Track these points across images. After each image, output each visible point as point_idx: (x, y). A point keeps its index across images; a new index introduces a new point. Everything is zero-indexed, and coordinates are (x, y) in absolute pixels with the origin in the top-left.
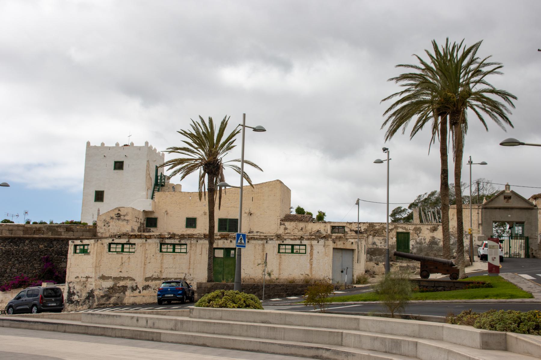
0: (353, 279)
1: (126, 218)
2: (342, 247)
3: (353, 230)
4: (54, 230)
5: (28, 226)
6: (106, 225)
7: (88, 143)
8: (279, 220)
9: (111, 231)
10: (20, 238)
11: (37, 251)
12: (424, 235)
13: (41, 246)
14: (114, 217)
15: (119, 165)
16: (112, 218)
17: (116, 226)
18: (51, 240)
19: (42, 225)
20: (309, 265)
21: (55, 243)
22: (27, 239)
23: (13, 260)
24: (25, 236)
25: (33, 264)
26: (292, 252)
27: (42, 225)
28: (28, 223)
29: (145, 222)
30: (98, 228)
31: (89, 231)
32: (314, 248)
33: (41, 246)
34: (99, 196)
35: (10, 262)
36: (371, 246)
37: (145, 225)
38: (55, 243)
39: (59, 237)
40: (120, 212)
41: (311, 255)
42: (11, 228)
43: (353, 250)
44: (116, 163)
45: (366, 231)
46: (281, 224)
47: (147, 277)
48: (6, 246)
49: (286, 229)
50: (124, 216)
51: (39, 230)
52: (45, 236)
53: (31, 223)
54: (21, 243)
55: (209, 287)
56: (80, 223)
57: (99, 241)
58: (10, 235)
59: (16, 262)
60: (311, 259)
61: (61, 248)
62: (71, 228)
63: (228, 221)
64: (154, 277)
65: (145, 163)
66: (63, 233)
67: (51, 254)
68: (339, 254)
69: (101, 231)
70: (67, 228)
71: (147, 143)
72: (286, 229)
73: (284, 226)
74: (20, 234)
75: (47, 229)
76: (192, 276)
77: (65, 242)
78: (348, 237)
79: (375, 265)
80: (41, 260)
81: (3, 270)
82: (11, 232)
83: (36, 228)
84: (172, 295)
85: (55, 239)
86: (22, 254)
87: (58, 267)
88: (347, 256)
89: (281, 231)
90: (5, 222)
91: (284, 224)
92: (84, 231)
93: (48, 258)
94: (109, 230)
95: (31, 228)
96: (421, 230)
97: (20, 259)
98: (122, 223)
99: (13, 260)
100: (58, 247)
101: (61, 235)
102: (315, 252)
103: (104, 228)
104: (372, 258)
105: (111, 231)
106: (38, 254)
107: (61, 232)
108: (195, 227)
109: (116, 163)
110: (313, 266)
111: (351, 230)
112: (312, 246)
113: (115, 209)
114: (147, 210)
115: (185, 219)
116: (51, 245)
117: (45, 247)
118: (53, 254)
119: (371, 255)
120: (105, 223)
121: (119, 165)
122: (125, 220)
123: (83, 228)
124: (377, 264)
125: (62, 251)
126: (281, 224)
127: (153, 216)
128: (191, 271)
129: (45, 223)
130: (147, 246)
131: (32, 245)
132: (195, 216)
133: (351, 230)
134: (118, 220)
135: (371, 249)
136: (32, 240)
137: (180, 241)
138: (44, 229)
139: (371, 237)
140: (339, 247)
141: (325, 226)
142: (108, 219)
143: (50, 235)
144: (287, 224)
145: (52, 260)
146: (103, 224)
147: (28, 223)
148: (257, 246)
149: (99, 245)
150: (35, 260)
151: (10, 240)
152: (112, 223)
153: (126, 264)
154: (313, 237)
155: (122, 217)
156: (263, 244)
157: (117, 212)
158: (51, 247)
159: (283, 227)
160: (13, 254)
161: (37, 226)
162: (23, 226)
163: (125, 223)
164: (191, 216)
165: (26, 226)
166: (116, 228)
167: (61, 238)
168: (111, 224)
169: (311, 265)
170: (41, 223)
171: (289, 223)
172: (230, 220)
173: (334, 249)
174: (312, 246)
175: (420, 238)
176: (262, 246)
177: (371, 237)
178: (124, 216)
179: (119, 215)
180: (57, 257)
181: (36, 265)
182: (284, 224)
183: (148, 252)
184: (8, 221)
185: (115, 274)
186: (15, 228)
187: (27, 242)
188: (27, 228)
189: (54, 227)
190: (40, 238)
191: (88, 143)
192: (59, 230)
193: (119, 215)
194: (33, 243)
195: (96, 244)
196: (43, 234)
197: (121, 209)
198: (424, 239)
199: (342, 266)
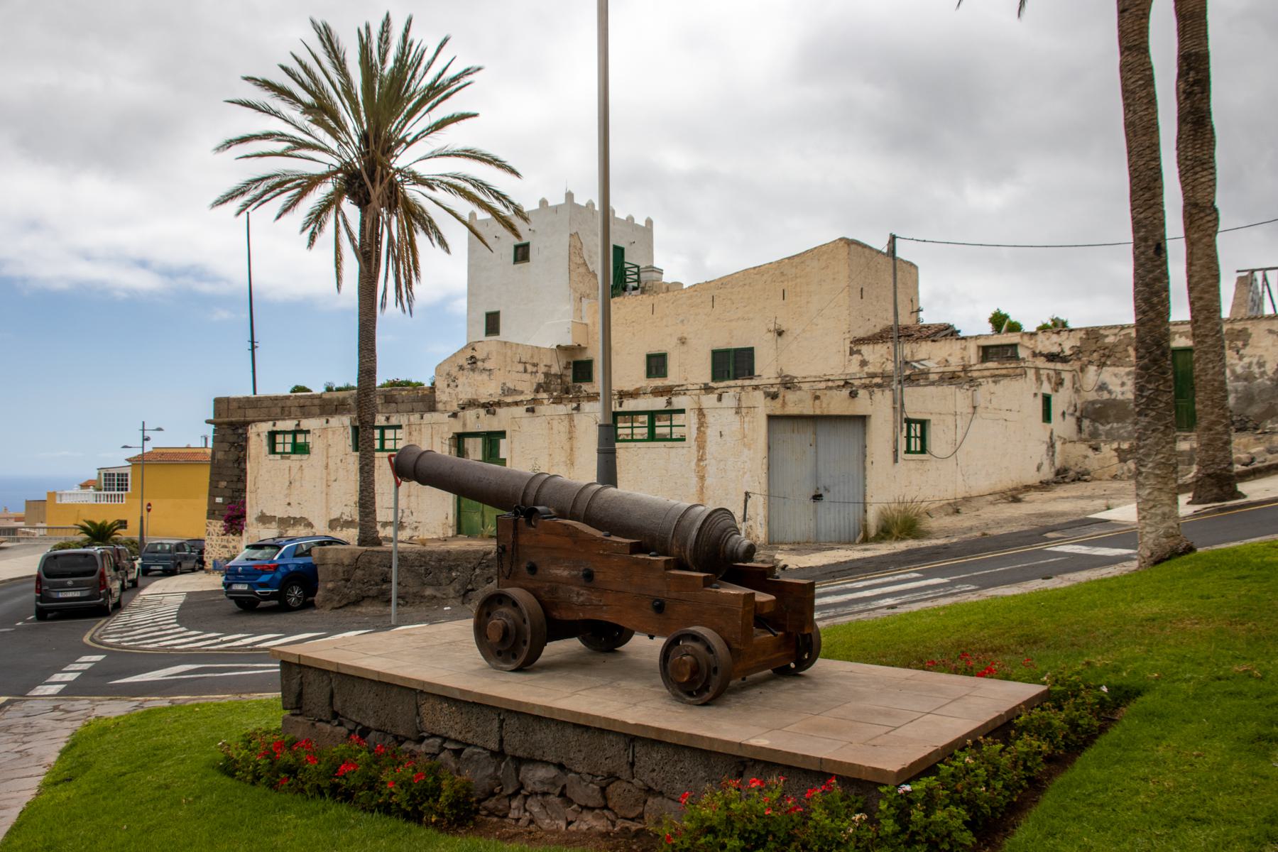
0: (865, 527)
1: (488, 365)
2: (808, 411)
3: (1041, 354)
6: (453, 384)
8: (848, 342)
12: (1259, 352)
16: (461, 368)
20: (694, 480)
26: (652, 437)
29: (570, 372)
30: (438, 393)
32: (710, 419)
34: (493, 323)
36: (1092, 396)
37: (570, 379)
40: (474, 354)
41: (701, 446)
43: (863, 420)
45: (1078, 352)
46: (851, 354)
47: (332, 517)
49: (864, 363)
50: (483, 361)
55: (346, 562)
56: (408, 383)
60: (701, 459)
62: (392, 396)
63: (732, 354)
64: (345, 517)
65: (566, 239)
68: (798, 442)
70: (386, 396)
71: (569, 196)
72: (864, 363)
73: (859, 357)
76: (414, 518)
78: (975, 374)
79: (1090, 453)
84: (245, 587)
88: (836, 444)
89: (854, 368)
91: (859, 352)
92: (414, 401)
94: (457, 395)
96: (1249, 335)
102: (711, 433)
103: (447, 390)
104: (1096, 429)
108: (664, 375)
110: (708, 481)
111: (1035, 355)
112: (701, 412)
114: (563, 344)
115: (644, 358)
119: (1093, 421)
123: (412, 394)
124: (1096, 449)
126: (851, 354)
127: (584, 357)
128: (413, 505)
130: (330, 436)
133: (1035, 355)
134: (473, 370)
135: (1093, 403)
137: (388, 419)
138: (350, 401)
139: (1092, 369)
140: (792, 410)
141: (965, 349)
142: (454, 371)
144: (866, 350)
148: (555, 423)
153: (297, 484)
154: (878, 380)
155: (479, 364)
156: (570, 416)
157: (469, 353)
159: (856, 358)
162: (320, 397)
163: (485, 376)
164: (655, 350)
166: (469, 389)
168: (459, 382)
169: (702, 478)
171: (871, 346)
172: (736, 350)
173: (771, 418)
174: (701, 412)
175: (1246, 360)
176: (566, 423)
177: (1092, 369)
178: (483, 361)
179: (473, 361)
182: (859, 352)
183: (332, 451)
185: (280, 513)
193: (473, 361)
197: (477, 347)
198: (1261, 365)
199: (816, 477)
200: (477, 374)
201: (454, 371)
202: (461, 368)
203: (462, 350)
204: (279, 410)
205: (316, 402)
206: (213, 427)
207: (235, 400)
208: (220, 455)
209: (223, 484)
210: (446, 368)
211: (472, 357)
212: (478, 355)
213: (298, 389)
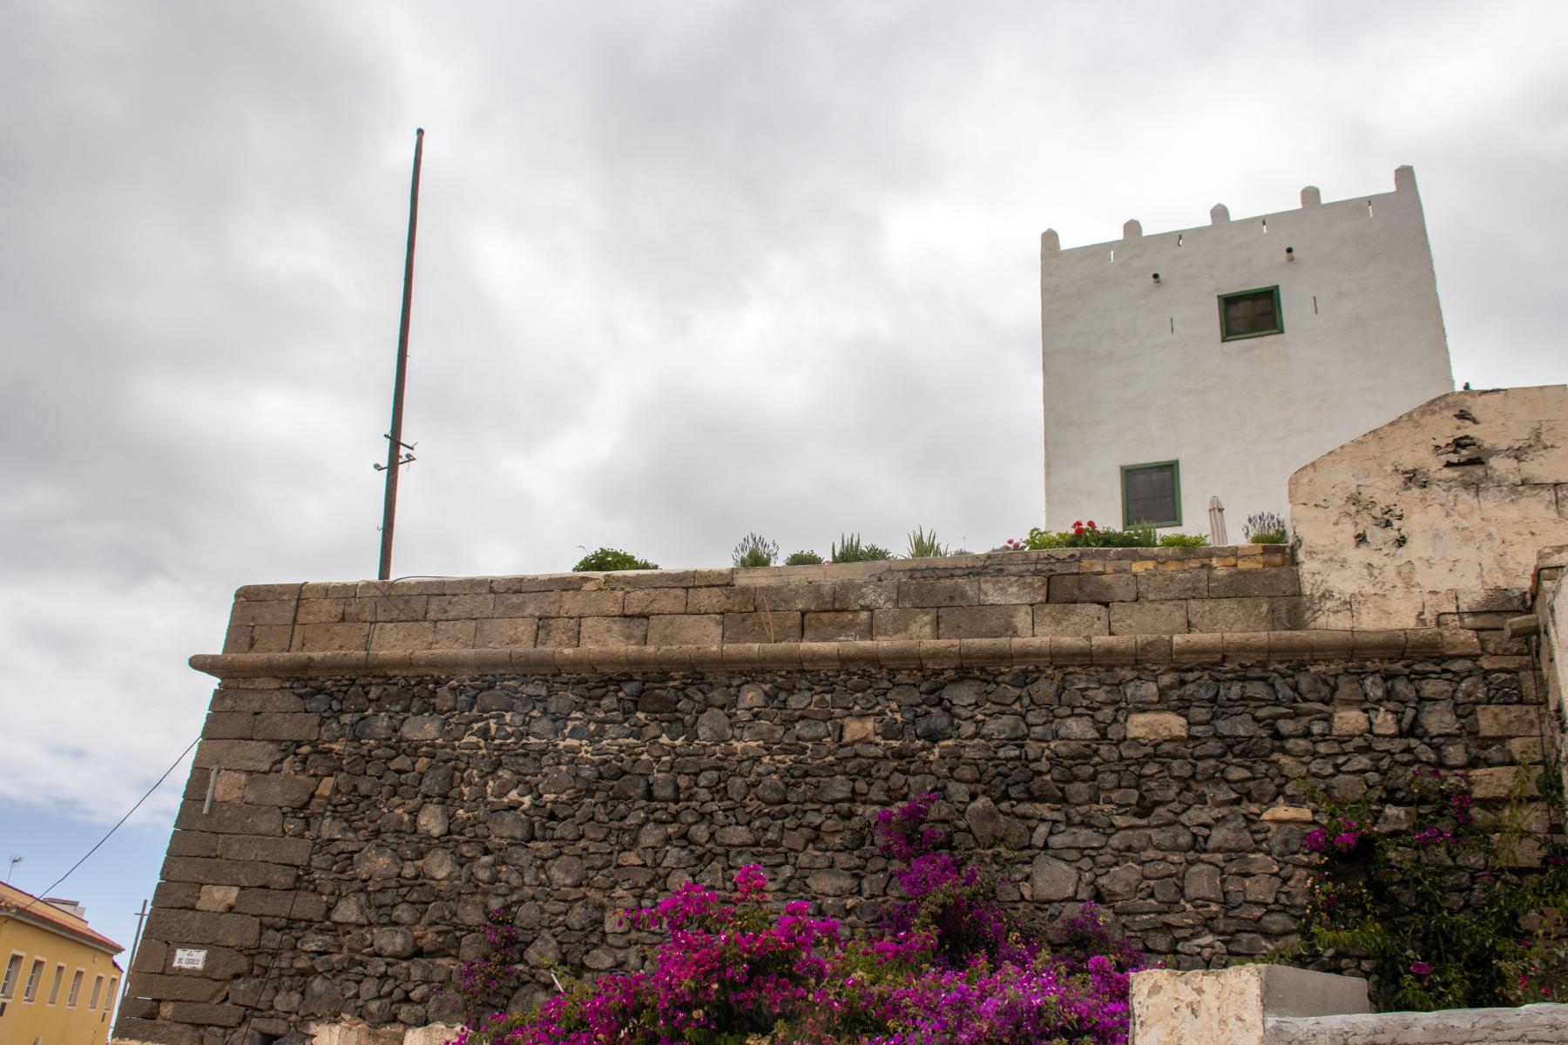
4: (954, 596)
5: (757, 579)
6: (1377, 535)
7: (1050, 238)
9: (1427, 579)
10: (697, 672)
11: (830, 770)
13: (855, 729)
14: (1434, 466)
15: (1251, 313)
16: (1413, 478)
17: (1466, 536)
18: (932, 679)
19: (856, 572)
21: (963, 696)
22: (753, 670)
23: (651, 835)
24: (732, 648)
25: (802, 874)
27: (856, 572)
28: (756, 560)
30: (1308, 567)
31: (1238, 588)
33: (855, 729)
35: (631, 858)
39: (1002, 642)
40: (1471, 430)
42: (637, 600)
44: (1228, 302)
48: (601, 734)
50: (1518, 454)
51: (834, 607)
52: (883, 643)
53: (779, 561)
54: (708, 705)
58: (632, 649)
59: (673, 855)
61: (1018, 741)
66: (1022, 620)
67: (941, 792)
69: (1343, 583)
74: (705, 638)
75: (900, 594)
77: (1044, 689)
80: (860, 839)
81: (577, 916)
82: (637, 628)
83: (815, 589)
85: (968, 669)
86: (719, 790)
87: (1007, 892)
90: (599, 568)
92: (1193, 593)
93: (915, 815)
95: (778, 596)
97: (700, 832)
98: (1512, 513)
99: (651, 835)
100: (992, 726)
105: (1427, 579)
106: (839, 787)
107: (1008, 611)
109: (1228, 302)
113: (1430, 408)
116: (939, 719)
117: (889, 732)
118: (959, 791)
120: (1366, 524)
125: (1024, 760)
129: (875, 555)
131: (788, 723)
134: (1475, 487)
136: (787, 676)
138: (871, 596)
142: (1383, 490)
143: (921, 636)
145: (948, 844)
146: (1348, 530)
147: (756, 560)
150: (816, 836)
151: (629, 688)
152: (1422, 517)
157: (1447, 429)
158: (933, 737)
160: (649, 795)
161: (830, 577)
162: (723, 582)
165: (742, 580)
166: (1467, 553)
170: (850, 555)
180: (990, 816)
181: (823, 883)
184: (626, 561)
187: (751, 696)
188: (738, 596)
189: (950, 572)
190: (845, 661)
191: (1050, 238)
192: (994, 598)
193: (1469, 459)
194: (796, 702)
196: (870, 631)
200: (1491, 505)
203: (1411, 419)
204: (525, 629)
205: (707, 599)
206: (213, 683)
207: (326, 591)
208: (224, 786)
209: (220, 896)
210: (1344, 478)
211: (1459, 444)
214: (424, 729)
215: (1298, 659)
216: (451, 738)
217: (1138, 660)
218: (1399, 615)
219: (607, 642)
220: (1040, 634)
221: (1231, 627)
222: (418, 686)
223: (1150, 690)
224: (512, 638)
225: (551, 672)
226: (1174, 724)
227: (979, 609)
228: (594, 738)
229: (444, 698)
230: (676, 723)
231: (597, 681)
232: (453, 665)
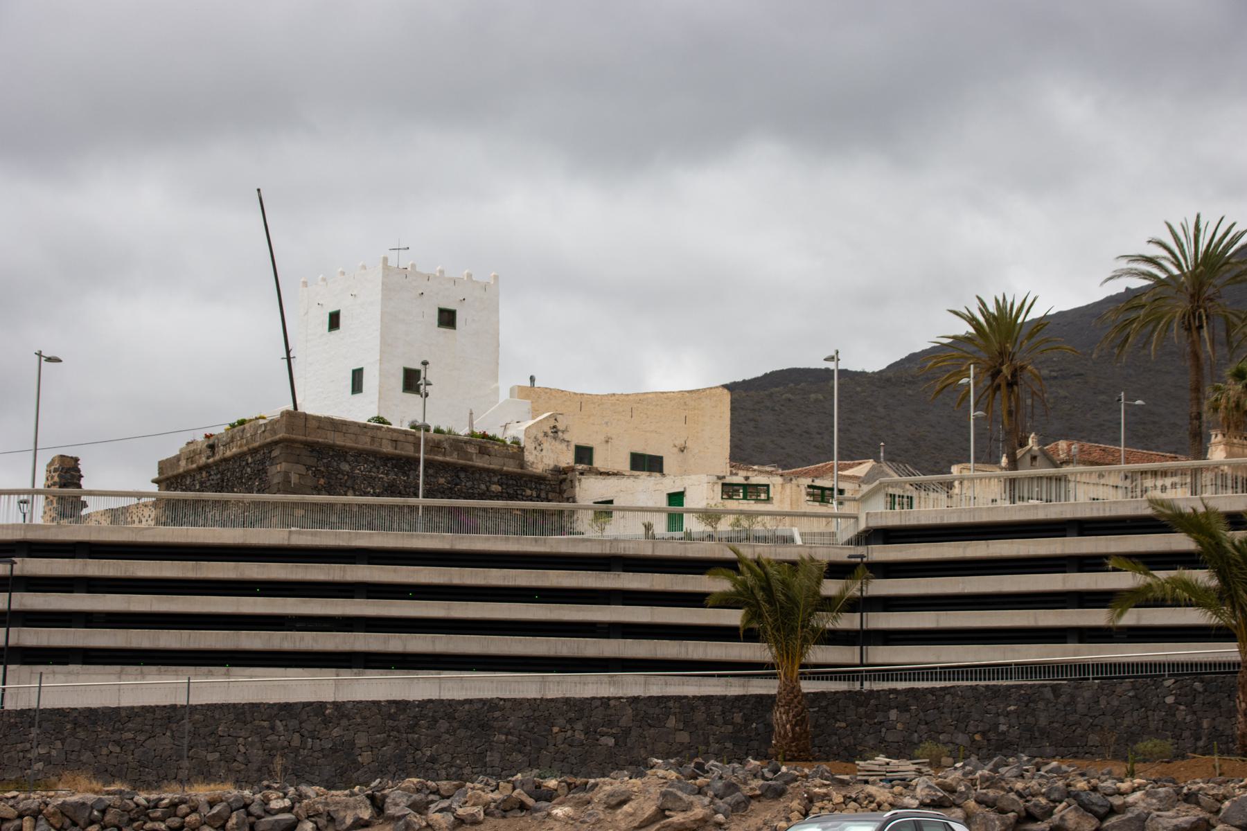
1: (566, 437)
14: (549, 432)
21: (462, 475)
30: (526, 453)
31: (513, 456)
33: (442, 481)
34: (412, 381)
38: (462, 475)
57: (794, 481)
70: (480, 447)
75: (451, 445)
85: (464, 469)
92: (505, 456)
101: (471, 459)
103: (535, 452)
105: (546, 461)
121: (447, 318)
122: (564, 440)
132: (590, 444)
134: (555, 438)
138: (446, 445)
149: (794, 488)
155: (560, 434)
157: (552, 423)
163: (564, 446)
167: (472, 467)
168: (545, 446)
184: (384, 423)
186: (402, 438)
193: (555, 430)
195: (788, 486)
197: (559, 418)
201: (540, 436)
202: (546, 434)
204: (368, 440)
210: (534, 432)
212: (560, 426)
213: (380, 420)
214: (345, 467)
215: (521, 476)
216: (353, 469)
217: (494, 472)
218: (539, 468)
219: (387, 449)
220: (479, 462)
221: (511, 467)
222: (341, 453)
223: (496, 479)
224: (364, 443)
225: (374, 454)
226: (499, 488)
227: (466, 453)
228: (387, 474)
229: (350, 458)
230: (405, 474)
231: (386, 459)
232: (351, 449)
